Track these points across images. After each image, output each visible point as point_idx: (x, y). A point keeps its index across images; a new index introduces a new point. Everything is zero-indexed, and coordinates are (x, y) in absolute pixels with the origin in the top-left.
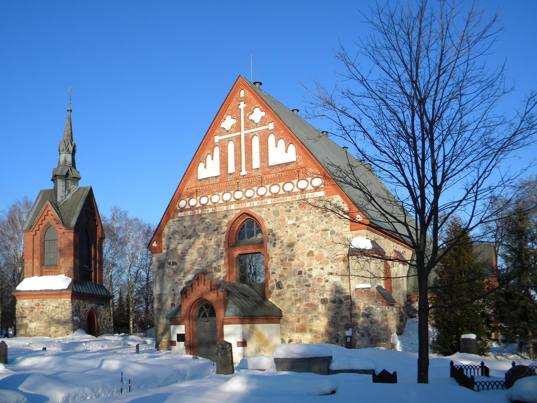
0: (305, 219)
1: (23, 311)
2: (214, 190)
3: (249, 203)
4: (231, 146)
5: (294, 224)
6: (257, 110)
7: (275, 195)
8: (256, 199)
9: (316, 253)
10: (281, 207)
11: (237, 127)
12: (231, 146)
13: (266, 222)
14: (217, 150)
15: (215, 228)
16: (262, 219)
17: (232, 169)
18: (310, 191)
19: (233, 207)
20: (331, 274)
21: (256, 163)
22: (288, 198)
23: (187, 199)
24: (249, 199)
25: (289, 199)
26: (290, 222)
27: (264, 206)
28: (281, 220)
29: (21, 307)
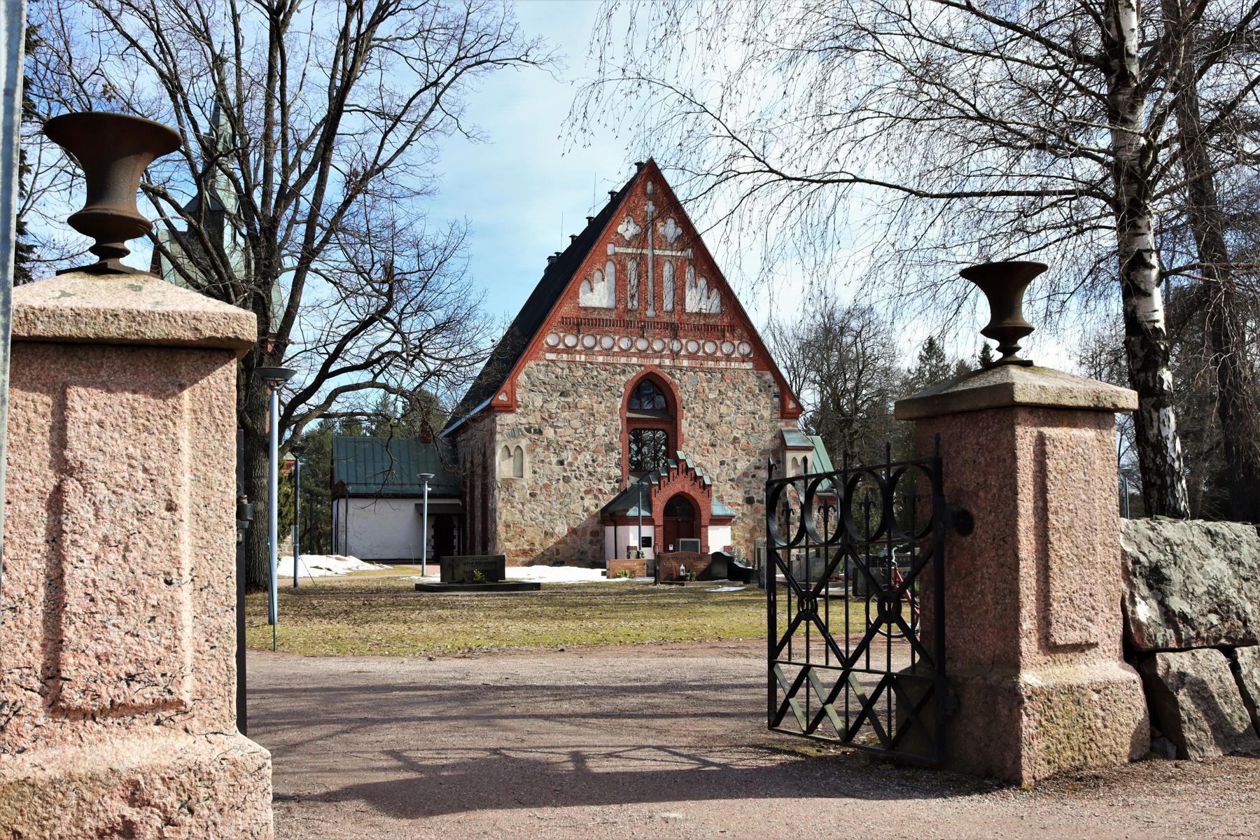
6: (671, 222)
9: (743, 441)
11: (640, 240)
14: (610, 268)
18: (736, 360)
19: (634, 360)
20: (757, 468)
21: (668, 305)
24: (658, 354)
25: (711, 364)
26: (711, 396)
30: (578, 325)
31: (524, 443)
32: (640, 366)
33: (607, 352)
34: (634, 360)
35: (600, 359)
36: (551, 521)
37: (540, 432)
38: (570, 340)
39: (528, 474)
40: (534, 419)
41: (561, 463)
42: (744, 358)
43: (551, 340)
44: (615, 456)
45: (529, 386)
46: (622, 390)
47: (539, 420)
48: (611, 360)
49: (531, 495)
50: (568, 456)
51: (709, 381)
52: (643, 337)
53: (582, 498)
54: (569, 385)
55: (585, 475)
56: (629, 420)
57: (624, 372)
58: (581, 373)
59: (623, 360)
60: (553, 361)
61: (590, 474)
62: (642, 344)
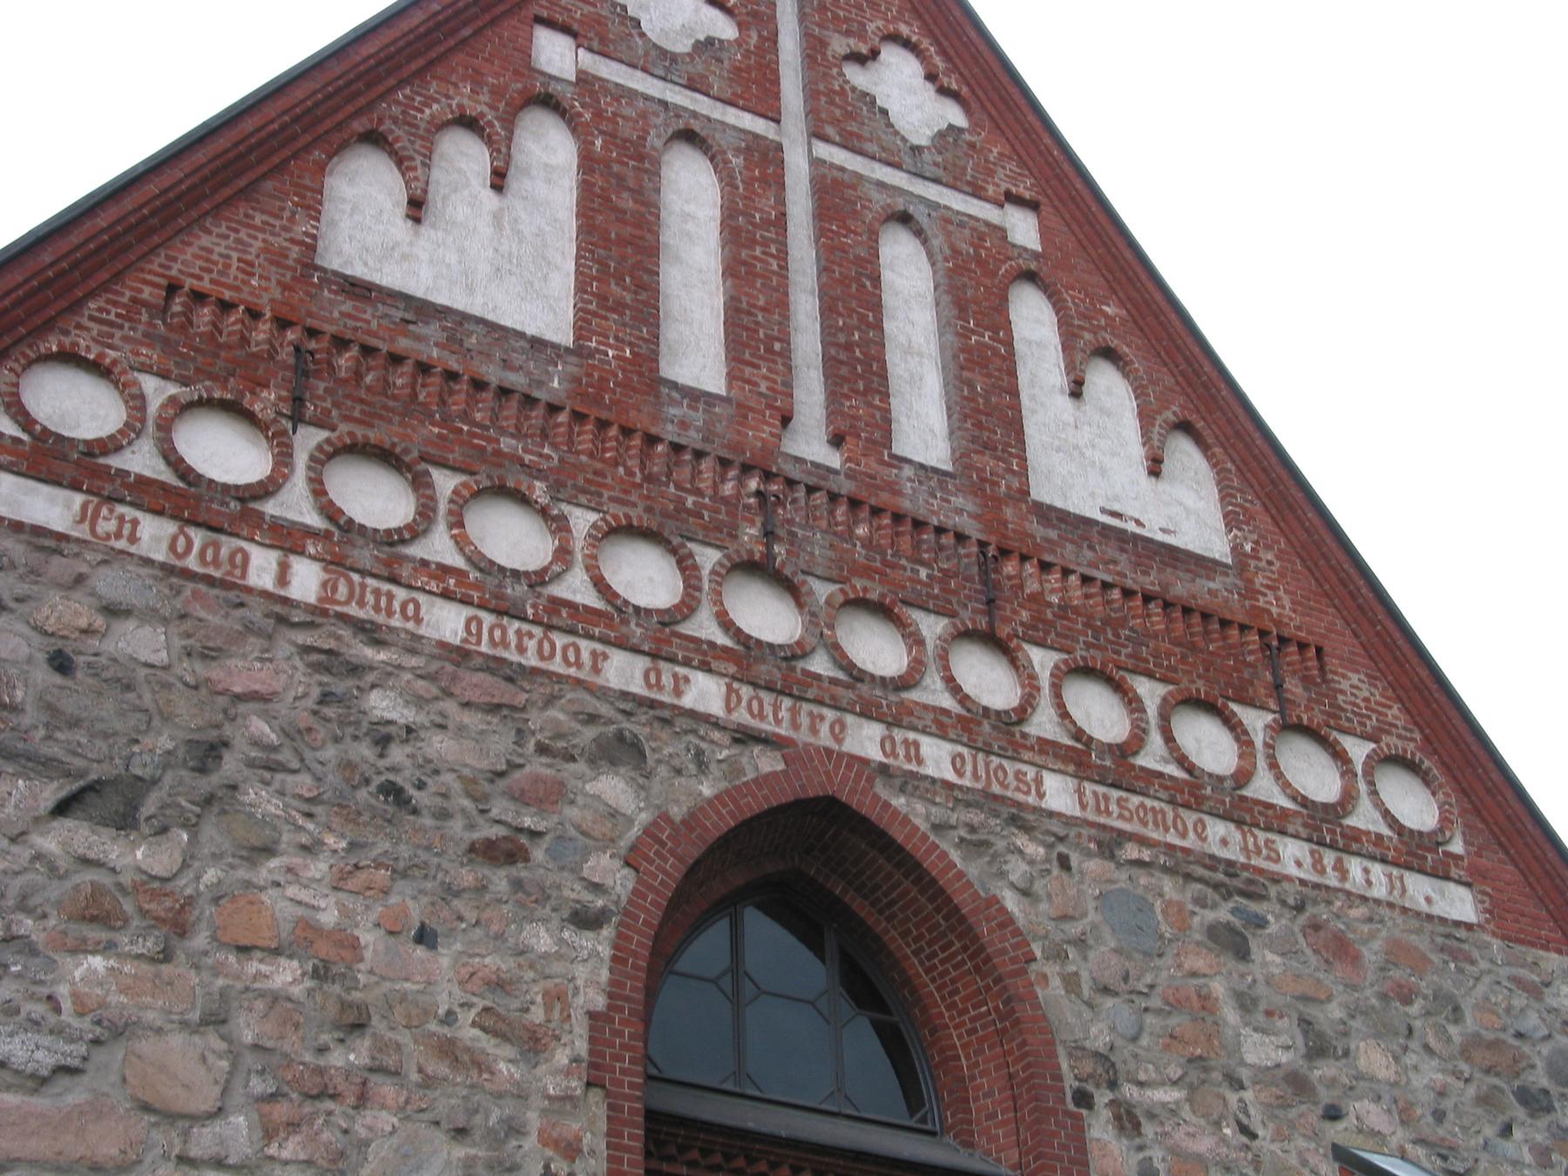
0: (1373, 1059)
2: (506, 444)
3: (874, 730)
4: (691, 195)
5: (1298, 1084)
7: (1111, 767)
8: (941, 725)
10: (1168, 885)
12: (691, 195)
13: (1052, 969)
14: (549, 150)
17: (696, 353)
19: (705, 692)
22: (1217, 829)
23: (156, 391)
25: (1221, 838)
26: (1263, 1050)
27: (1022, 818)
28: (1175, 1004)
30: (304, 368)
32: (745, 737)
33: (487, 588)
34: (705, 692)
35: (447, 622)
42: (1413, 852)
51: (1232, 943)
57: (622, 751)
59: (624, 671)
62: (767, 617)
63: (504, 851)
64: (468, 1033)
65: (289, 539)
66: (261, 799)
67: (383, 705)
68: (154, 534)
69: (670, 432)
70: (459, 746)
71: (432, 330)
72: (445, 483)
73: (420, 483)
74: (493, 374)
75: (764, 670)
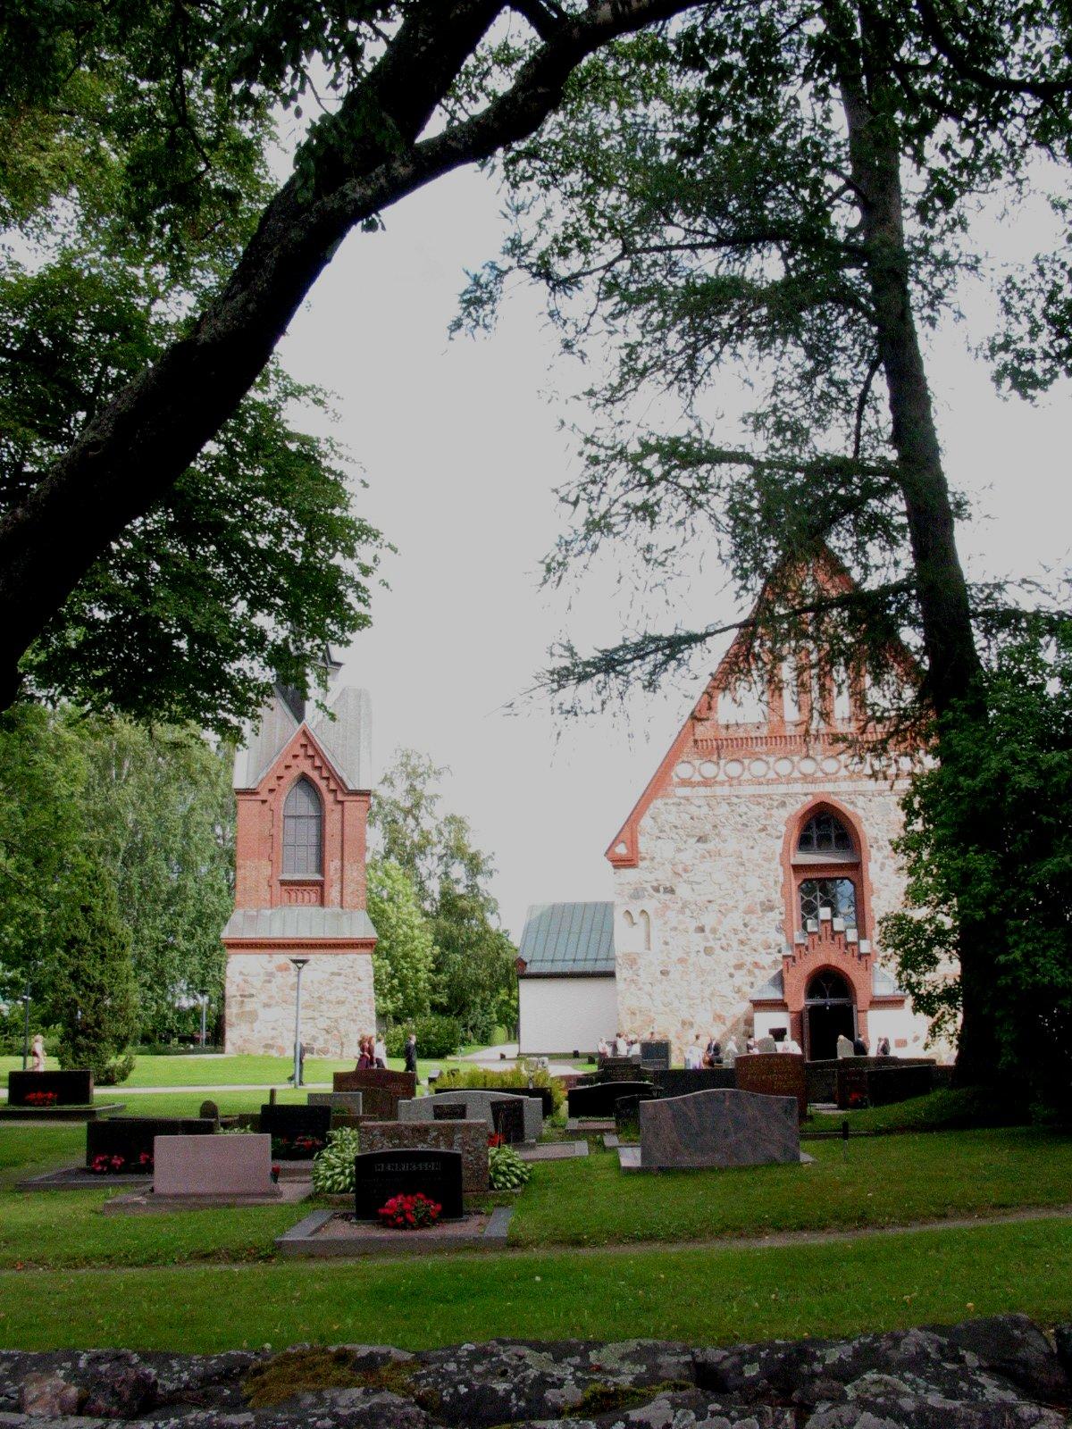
1: (246, 981)
15: (760, 827)
16: (857, 816)
19: (798, 788)
23: (697, 763)
29: (241, 973)
31: (650, 905)
32: (806, 795)
35: (749, 790)
36: (690, 1006)
37: (672, 891)
38: (709, 770)
39: (656, 944)
40: (663, 876)
41: (701, 929)
43: (682, 770)
44: (776, 917)
45: (656, 832)
46: (783, 829)
47: (670, 874)
48: (764, 790)
49: (662, 973)
50: (708, 920)
52: (808, 756)
53: (731, 976)
54: (708, 827)
55: (735, 944)
56: (797, 868)
57: (783, 804)
58: (724, 808)
60: (687, 799)
61: (742, 942)
63: (764, 829)
64: (760, 861)
65: (722, 783)
66: (725, 832)
67: (743, 809)
68: (702, 791)
69: (788, 734)
70: (759, 810)
71: (741, 730)
72: (746, 762)
73: (742, 763)
74: (753, 735)
75: (809, 779)
